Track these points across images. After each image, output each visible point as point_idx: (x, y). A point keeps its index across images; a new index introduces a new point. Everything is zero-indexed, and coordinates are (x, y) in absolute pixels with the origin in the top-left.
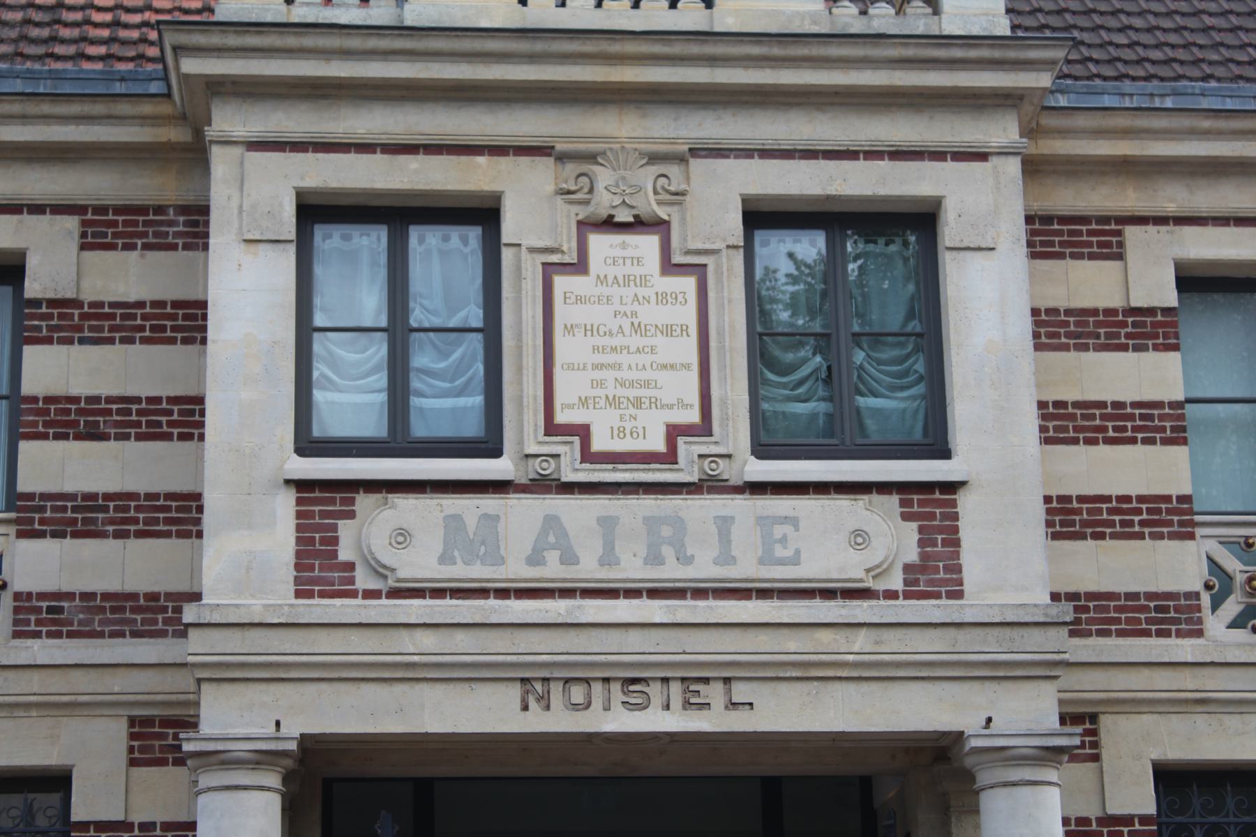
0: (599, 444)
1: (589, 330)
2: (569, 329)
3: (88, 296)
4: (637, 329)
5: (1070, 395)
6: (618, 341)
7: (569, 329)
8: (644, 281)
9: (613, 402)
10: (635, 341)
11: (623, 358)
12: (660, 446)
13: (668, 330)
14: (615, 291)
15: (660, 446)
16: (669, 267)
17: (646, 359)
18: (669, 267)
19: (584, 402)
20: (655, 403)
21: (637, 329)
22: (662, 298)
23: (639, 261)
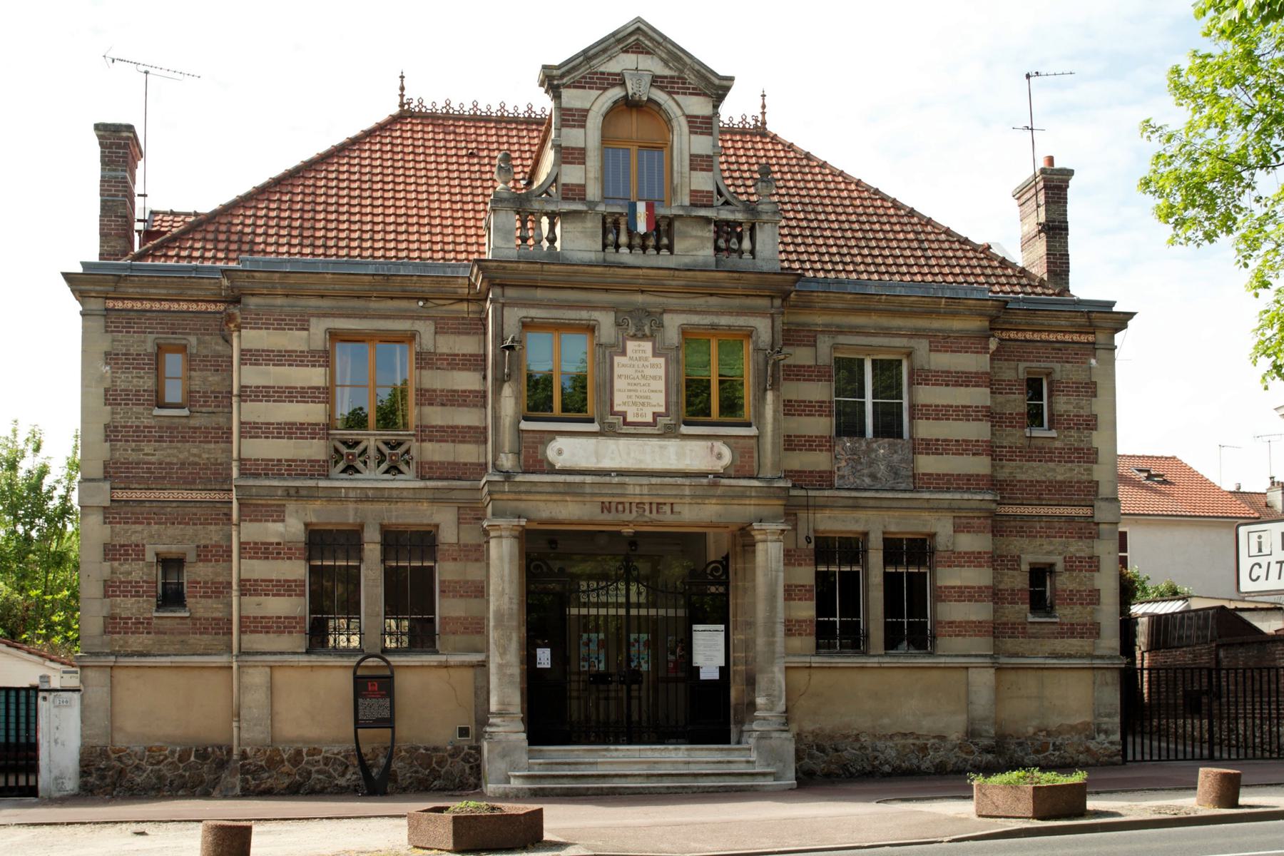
0: (629, 419)
1: (627, 377)
2: (620, 377)
3: (439, 351)
4: (643, 377)
5: (794, 398)
6: (636, 381)
7: (620, 377)
8: (646, 359)
9: (634, 404)
10: (643, 382)
11: (638, 388)
12: (649, 419)
13: (654, 378)
14: (636, 363)
15: (649, 419)
16: (655, 354)
17: (646, 388)
18: (655, 354)
19: (624, 404)
20: (649, 404)
21: (643, 377)
22: (653, 366)
23: (644, 351)
